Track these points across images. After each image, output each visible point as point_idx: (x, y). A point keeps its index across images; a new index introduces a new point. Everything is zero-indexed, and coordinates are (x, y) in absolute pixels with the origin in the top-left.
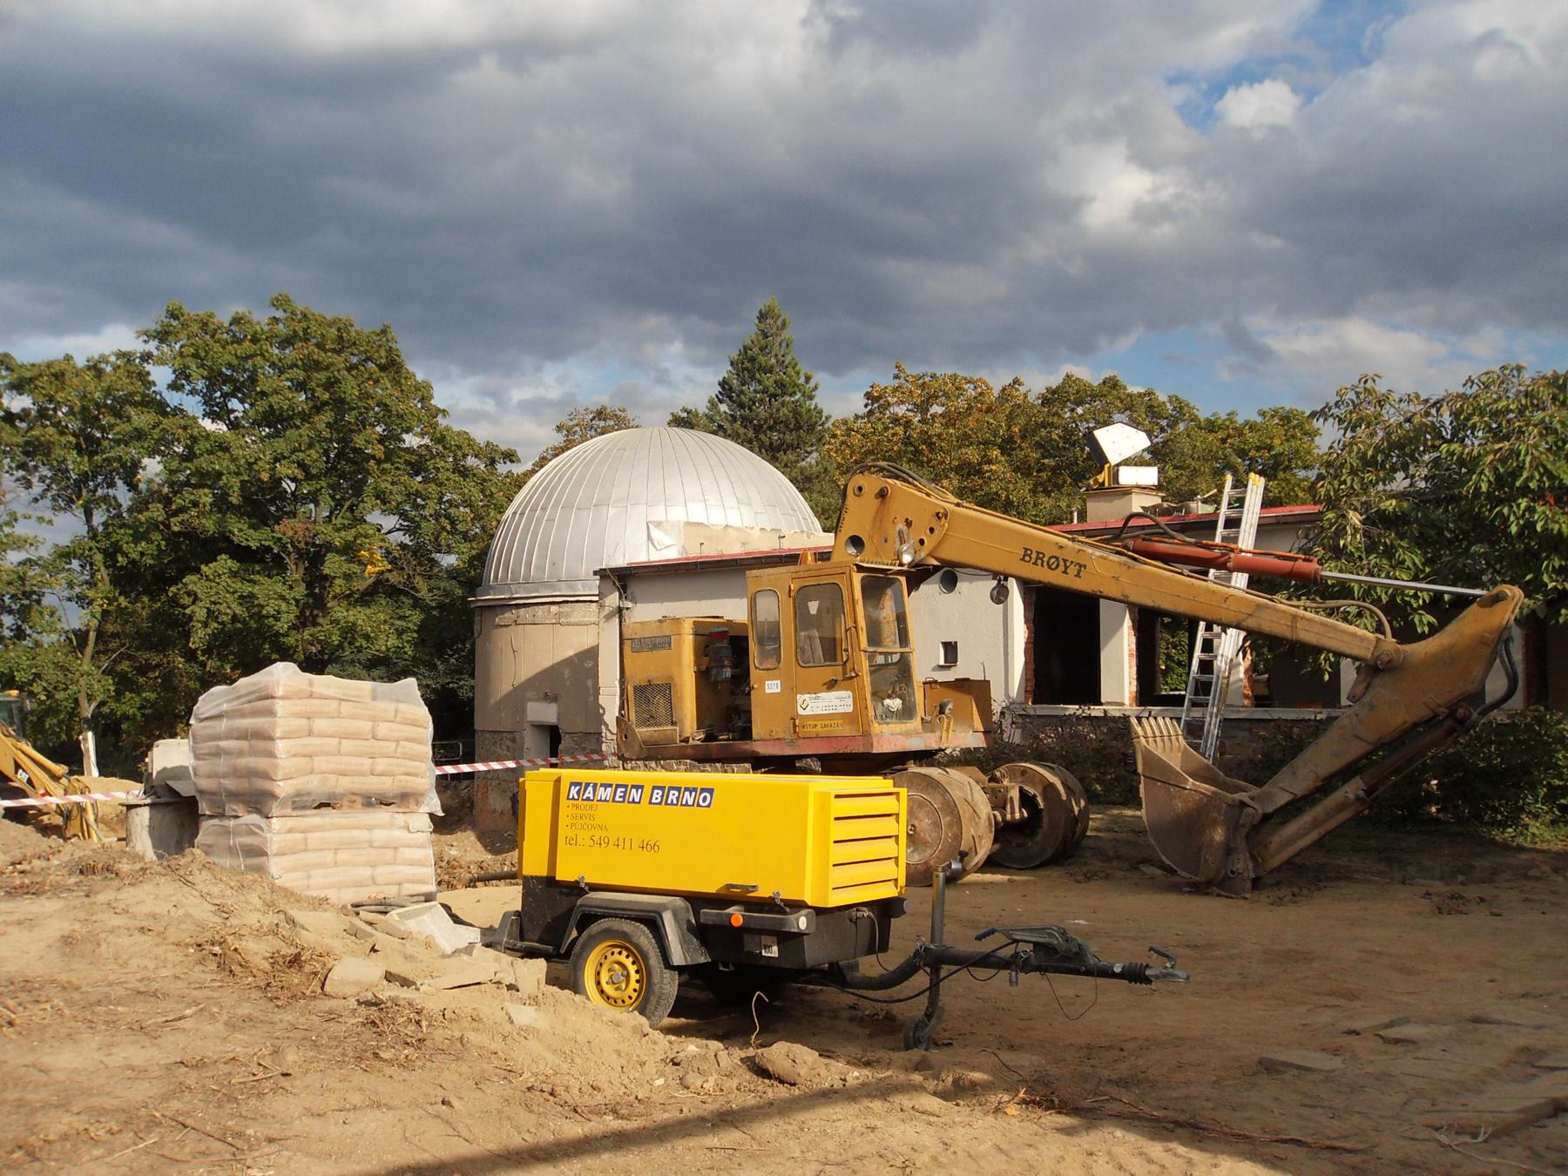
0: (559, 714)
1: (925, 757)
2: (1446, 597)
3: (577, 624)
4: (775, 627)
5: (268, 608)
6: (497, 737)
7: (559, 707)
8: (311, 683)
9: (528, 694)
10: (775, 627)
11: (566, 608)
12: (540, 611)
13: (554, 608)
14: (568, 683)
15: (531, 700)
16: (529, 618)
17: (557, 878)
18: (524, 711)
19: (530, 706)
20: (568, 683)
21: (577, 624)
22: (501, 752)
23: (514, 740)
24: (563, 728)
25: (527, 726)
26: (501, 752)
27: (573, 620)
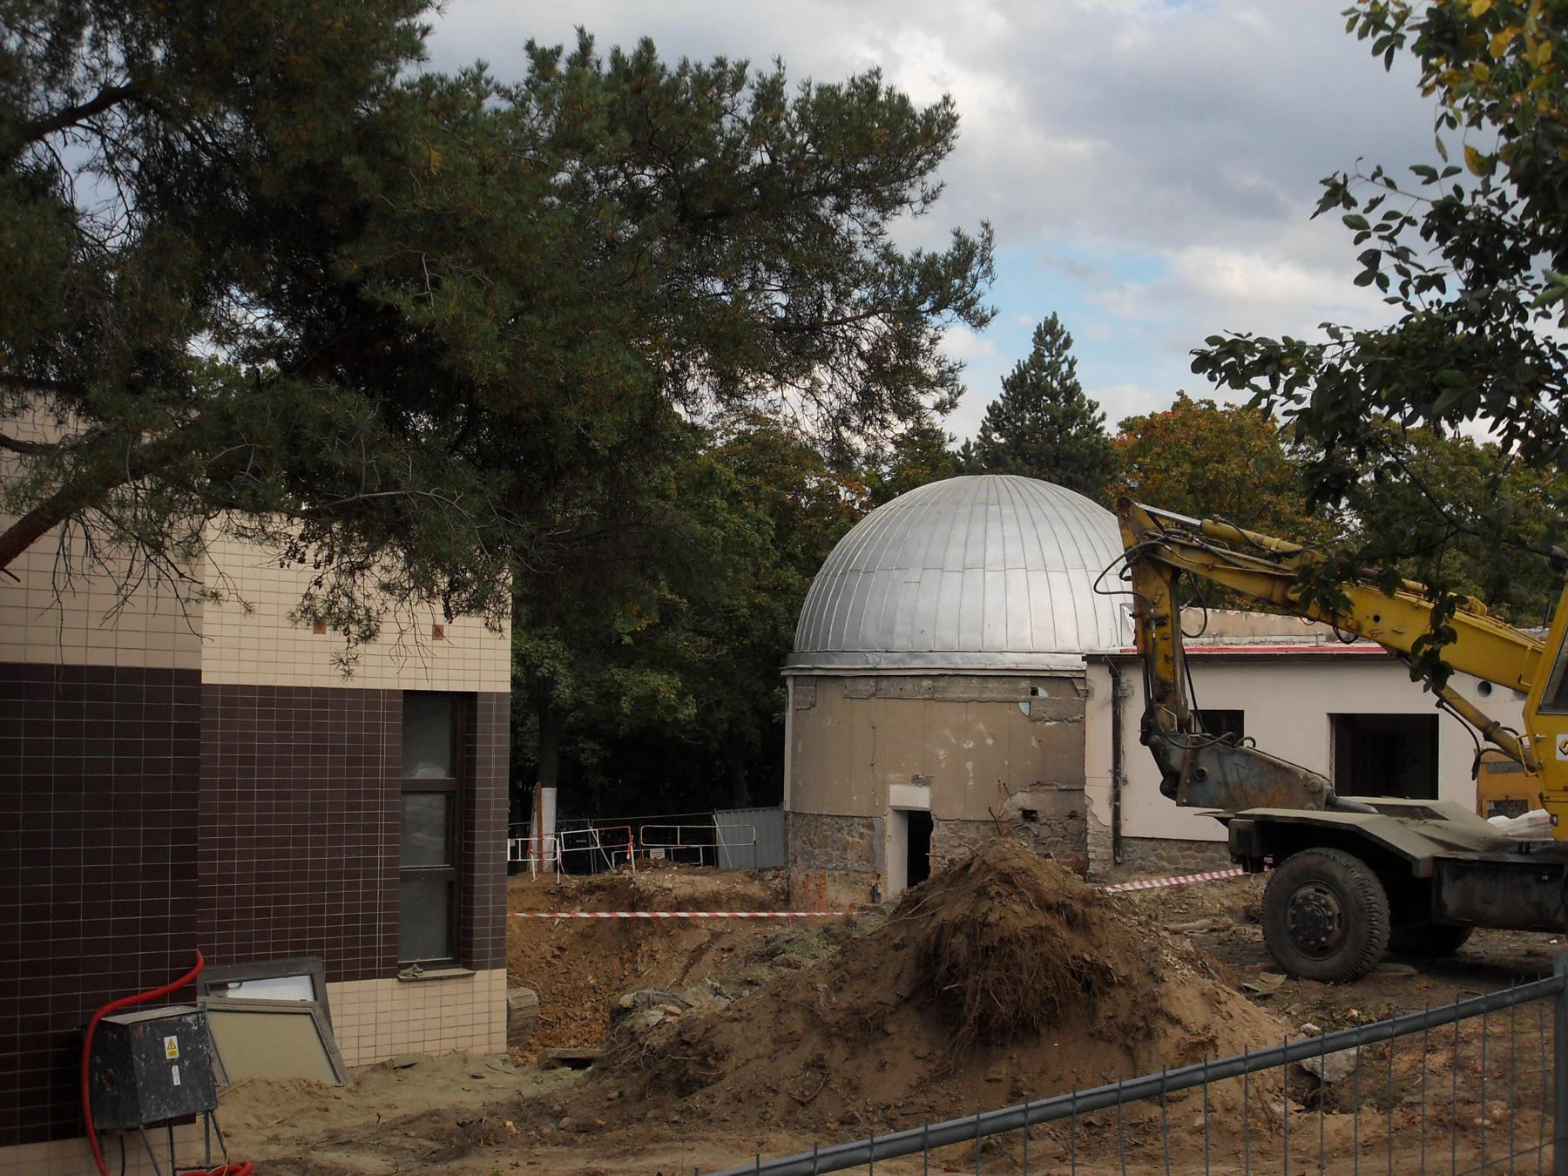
0: (932, 799)
1: (172, 565)
2: (382, 503)
3: (952, 701)
4: (1346, 727)
5: (542, 669)
6: (843, 823)
7: (932, 792)
8: (344, 663)
9: (892, 776)
10: (1346, 727)
11: (941, 683)
12: (909, 686)
13: (926, 683)
14: (943, 765)
15: (895, 782)
16: (894, 692)
17: (206, 679)
18: (886, 794)
19: (893, 788)
20: (943, 765)
21: (952, 701)
22: (850, 839)
23: (871, 827)
24: (937, 813)
25: (889, 810)
26: (850, 839)
27: (949, 696)
